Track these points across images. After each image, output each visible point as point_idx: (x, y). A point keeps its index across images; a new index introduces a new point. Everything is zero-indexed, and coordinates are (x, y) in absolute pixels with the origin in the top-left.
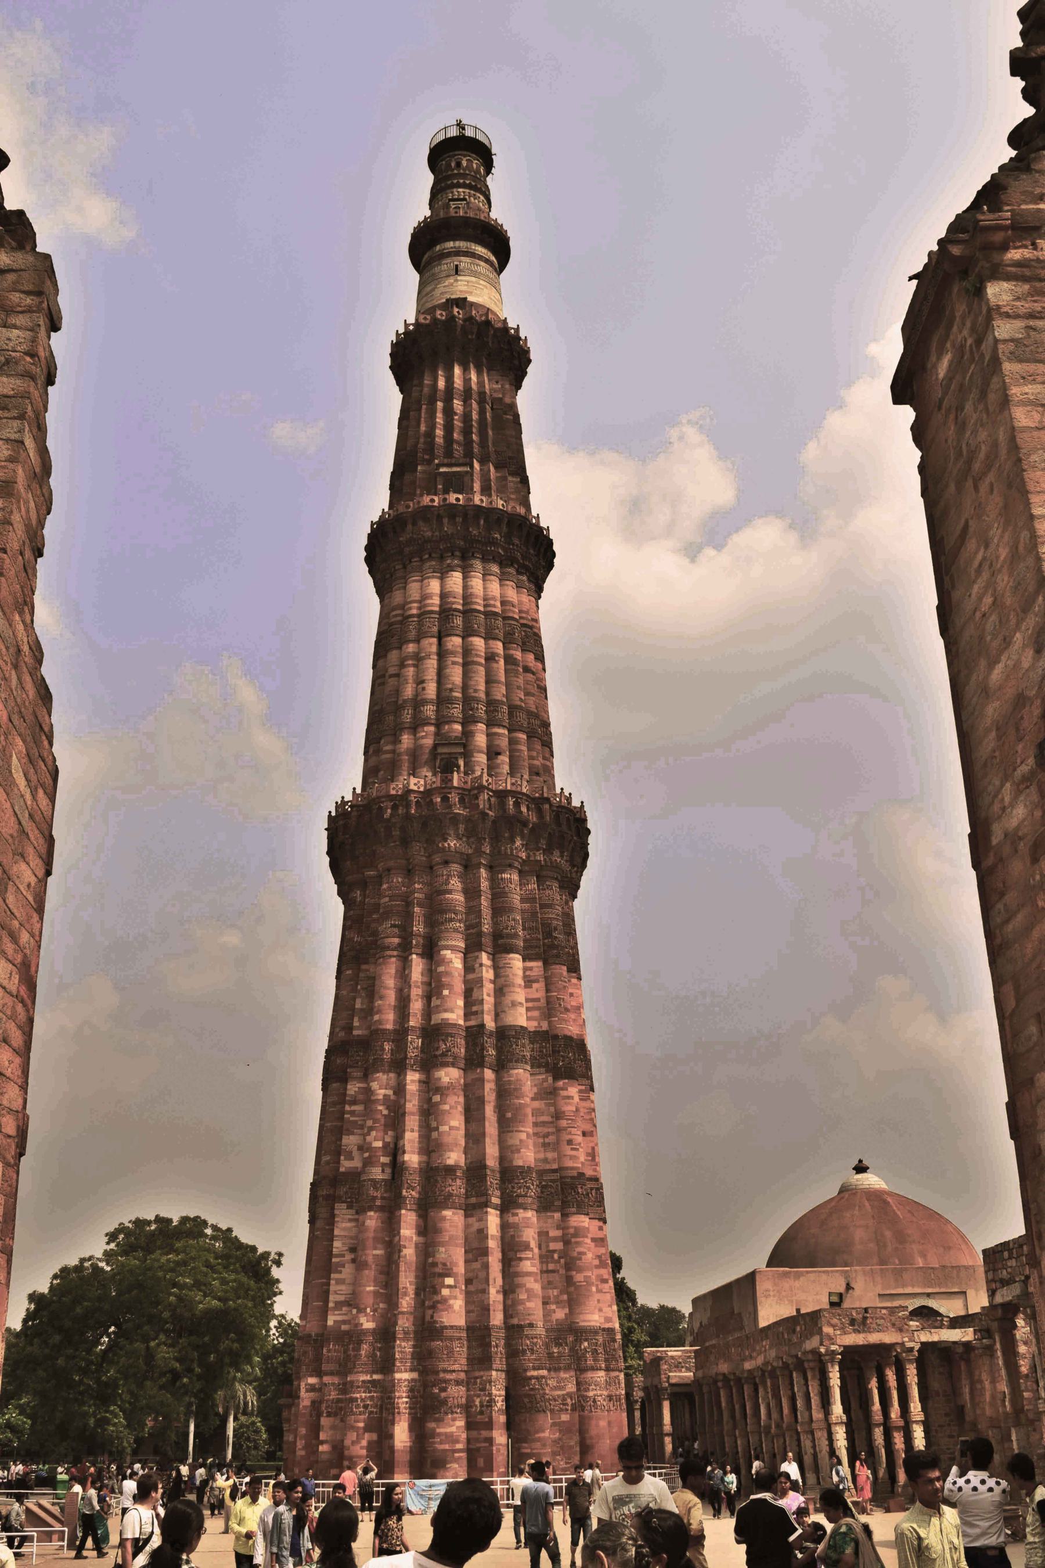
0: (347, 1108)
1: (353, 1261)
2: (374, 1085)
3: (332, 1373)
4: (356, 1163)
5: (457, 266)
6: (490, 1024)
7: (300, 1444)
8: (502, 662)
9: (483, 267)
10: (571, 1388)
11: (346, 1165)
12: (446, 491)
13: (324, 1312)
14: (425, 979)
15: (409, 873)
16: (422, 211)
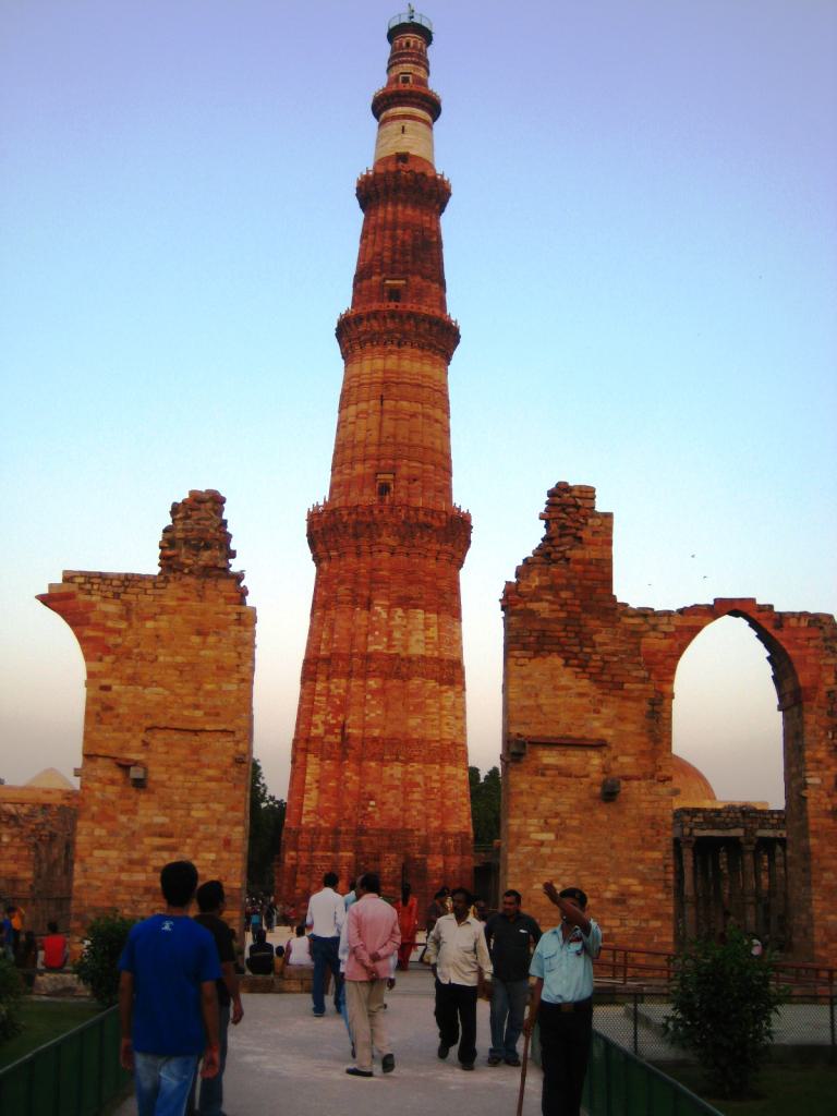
0: (316, 698)
1: (318, 788)
2: (332, 687)
3: (304, 850)
4: (320, 731)
5: (403, 127)
6: (403, 654)
7: (285, 888)
8: (420, 417)
9: (422, 126)
10: (441, 865)
11: (314, 732)
12: (390, 301)
13: (300, 815)
14: (365, 623)
15: (358, 554)
16: (379, 81)
